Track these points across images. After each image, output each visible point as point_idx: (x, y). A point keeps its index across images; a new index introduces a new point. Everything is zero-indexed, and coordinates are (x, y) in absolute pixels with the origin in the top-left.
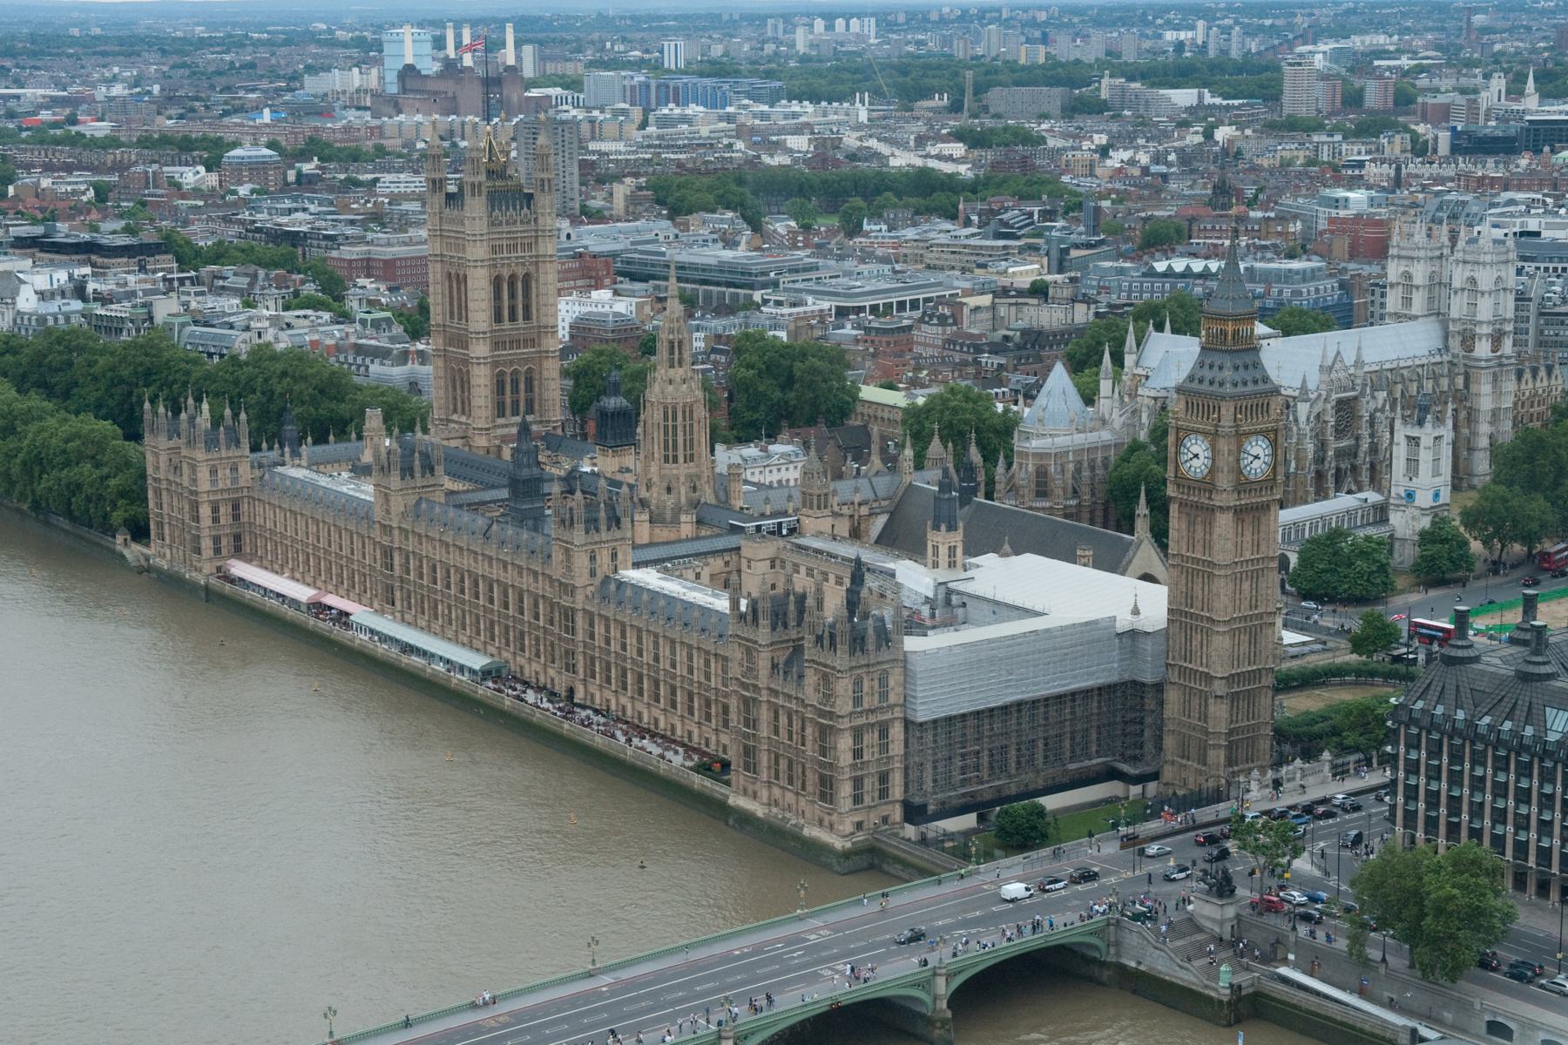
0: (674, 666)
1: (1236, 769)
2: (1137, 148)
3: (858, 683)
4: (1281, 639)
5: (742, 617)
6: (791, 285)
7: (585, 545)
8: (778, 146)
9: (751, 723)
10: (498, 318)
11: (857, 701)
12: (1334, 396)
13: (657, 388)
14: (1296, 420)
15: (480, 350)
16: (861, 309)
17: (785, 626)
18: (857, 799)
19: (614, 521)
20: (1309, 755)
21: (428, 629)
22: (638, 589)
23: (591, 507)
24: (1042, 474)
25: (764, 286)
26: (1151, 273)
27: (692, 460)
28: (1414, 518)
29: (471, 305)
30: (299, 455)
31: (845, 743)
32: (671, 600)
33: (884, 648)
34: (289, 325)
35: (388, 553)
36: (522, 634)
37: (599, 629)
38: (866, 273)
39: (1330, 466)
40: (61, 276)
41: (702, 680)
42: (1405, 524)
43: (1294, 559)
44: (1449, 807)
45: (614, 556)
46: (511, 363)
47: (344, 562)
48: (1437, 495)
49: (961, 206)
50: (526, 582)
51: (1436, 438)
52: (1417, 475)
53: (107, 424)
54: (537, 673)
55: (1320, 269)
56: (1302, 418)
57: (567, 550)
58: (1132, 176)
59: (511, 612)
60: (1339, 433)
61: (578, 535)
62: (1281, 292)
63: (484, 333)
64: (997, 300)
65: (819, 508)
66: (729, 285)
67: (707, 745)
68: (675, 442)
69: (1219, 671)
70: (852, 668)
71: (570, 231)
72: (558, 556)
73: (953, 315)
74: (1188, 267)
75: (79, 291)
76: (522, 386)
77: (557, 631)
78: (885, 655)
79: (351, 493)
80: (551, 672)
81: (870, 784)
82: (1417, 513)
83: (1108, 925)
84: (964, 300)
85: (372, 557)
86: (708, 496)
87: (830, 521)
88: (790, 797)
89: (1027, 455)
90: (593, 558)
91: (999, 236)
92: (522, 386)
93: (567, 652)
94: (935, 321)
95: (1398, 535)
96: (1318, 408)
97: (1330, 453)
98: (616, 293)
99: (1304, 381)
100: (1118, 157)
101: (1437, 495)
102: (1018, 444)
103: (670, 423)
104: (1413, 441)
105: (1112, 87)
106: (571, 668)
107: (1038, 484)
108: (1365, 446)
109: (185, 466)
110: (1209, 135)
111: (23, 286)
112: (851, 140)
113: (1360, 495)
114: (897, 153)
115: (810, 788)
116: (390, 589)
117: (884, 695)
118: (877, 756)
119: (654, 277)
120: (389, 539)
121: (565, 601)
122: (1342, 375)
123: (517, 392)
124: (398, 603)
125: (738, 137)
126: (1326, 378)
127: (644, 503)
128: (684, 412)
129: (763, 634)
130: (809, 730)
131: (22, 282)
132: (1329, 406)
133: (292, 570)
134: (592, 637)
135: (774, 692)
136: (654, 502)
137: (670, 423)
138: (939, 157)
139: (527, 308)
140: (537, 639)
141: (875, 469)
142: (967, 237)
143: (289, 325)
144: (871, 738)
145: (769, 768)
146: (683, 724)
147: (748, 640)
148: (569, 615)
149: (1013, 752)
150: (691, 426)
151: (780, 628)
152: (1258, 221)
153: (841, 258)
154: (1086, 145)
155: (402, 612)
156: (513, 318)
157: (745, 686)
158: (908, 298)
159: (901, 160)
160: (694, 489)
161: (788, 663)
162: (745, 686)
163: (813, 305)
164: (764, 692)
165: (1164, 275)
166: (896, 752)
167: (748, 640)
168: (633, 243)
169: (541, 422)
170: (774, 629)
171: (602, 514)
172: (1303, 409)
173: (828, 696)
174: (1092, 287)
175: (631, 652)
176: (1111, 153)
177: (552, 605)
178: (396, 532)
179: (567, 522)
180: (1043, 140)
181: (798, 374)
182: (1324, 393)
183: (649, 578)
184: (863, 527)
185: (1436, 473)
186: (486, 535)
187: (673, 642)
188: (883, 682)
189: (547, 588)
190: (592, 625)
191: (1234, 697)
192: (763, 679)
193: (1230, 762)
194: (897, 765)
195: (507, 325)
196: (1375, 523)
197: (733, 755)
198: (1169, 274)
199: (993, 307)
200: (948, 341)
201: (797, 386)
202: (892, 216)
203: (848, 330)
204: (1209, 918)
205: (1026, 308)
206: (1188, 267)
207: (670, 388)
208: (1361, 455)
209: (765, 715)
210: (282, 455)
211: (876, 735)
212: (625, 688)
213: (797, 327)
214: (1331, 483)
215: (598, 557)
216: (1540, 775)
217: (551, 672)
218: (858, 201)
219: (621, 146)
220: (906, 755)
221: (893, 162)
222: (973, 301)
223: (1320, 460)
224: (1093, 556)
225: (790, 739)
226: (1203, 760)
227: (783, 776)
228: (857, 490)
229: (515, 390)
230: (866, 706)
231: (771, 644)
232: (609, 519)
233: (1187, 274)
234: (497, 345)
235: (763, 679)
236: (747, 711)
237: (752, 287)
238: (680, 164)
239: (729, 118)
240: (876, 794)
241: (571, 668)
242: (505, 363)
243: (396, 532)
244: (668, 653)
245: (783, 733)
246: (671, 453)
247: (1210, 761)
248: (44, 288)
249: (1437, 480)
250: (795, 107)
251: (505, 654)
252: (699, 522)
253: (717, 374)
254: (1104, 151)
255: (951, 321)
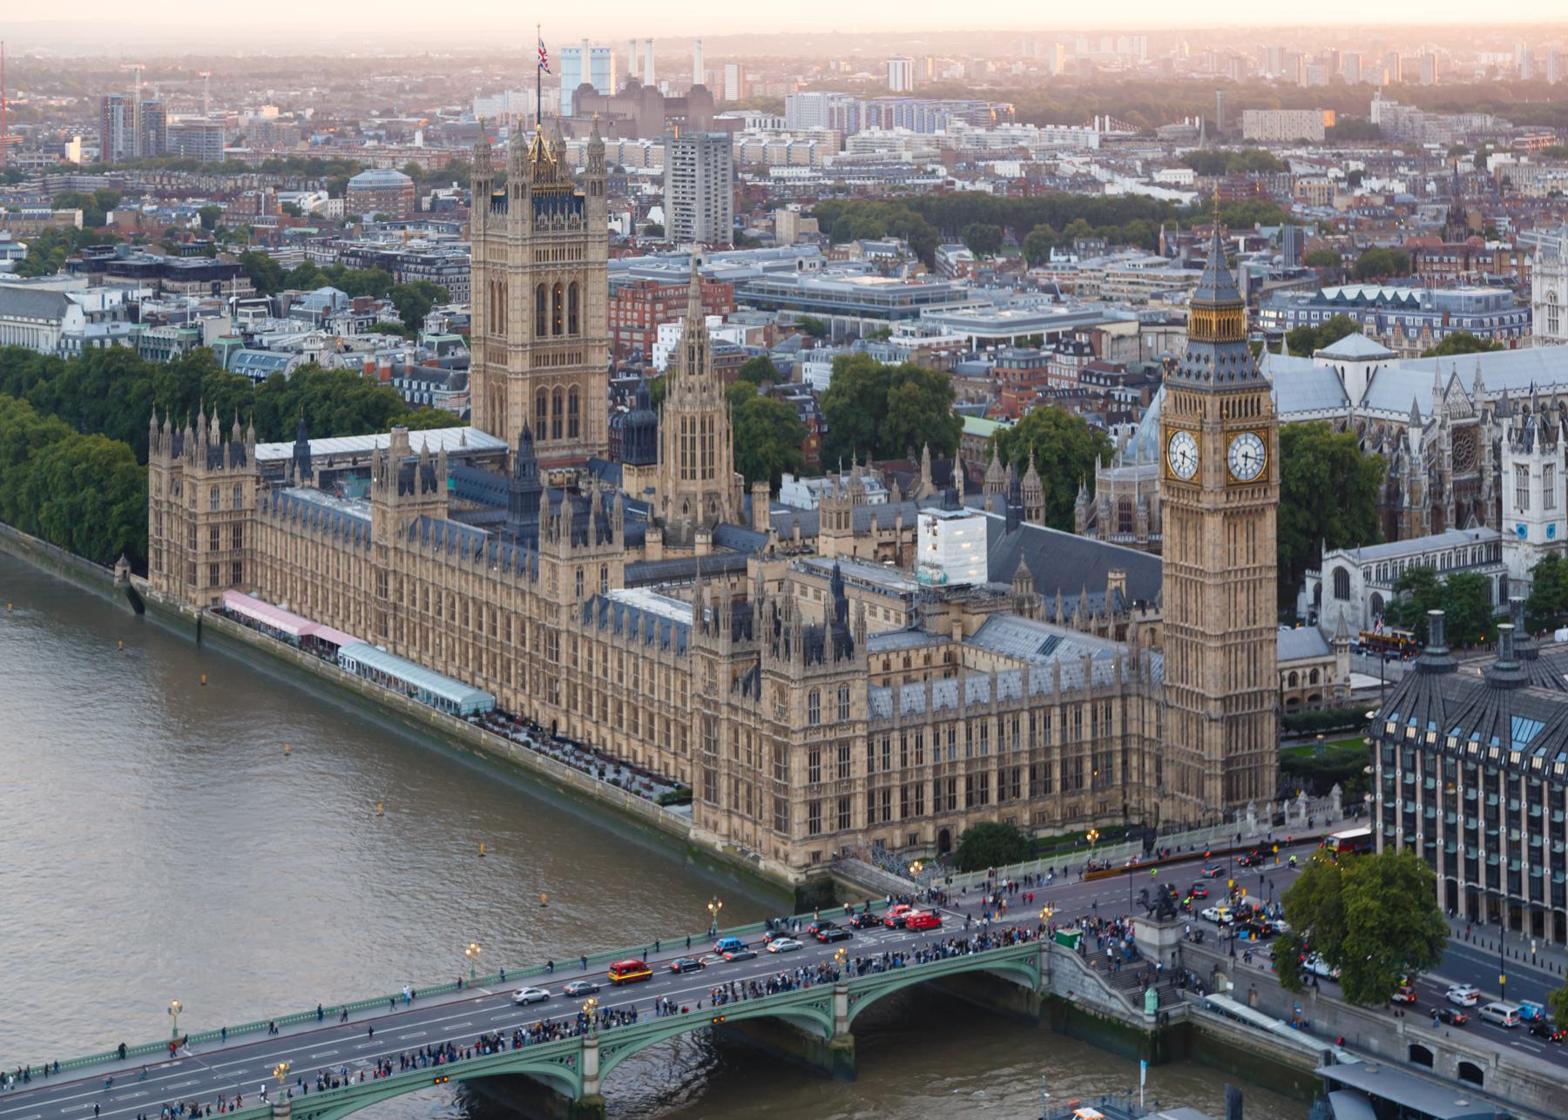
0: (652, 690)
1: (1238, 803)
2: (1392, 177)
3: (814, 697)
4: (1347, 679)
5: (705, 626)
6: (929, 315)
7: (571, 559)
8: (972, 173)
9: (712, 744)
10: (541, 330)
11: (814, 715)
12: (1449, 422)
13: (675, 396)
14: (1408, 448)
15: (518, 363)
16: (1006, 341)
17: (749, 637)
18: (814, 826)
19: (606, 534)
20: (1321, 791)
21: (418, 662)
22: (620, 606)
23: (580, 518)
24: (1125, 508)
25: (903, 316)
26: (1320, 300)
27: (712, 476)
28: (1527, 556)
29: (510, 315)
30: (311, 475)
31: (798, 762)
32: (650, 617)
33: (844, 658)
34: (347, 349)
35: (382, 576)
36: (509, 661)
37: (582, 653)
38: (1021, 302)
39: (1449, 503)
40: (115, 297)
41: (679, 704)
42: (1519, 561)
43: (1387, 596)
44: (1425, 832)
45: (604, 574)
46: (554, 379)
47: (340, 590)
48: (1551, 531)
49: (1162, 236)
50: (514, 603)
51: (1548, 466)
52: (1527, 507)
53: (117, 443)
54: (522, 706)
55: (1506, 297)
56: (1415, 446)
57: (553, 565)
58: (1373, 207)
59: (498, 638)
60: (1459, 463)
61: (563, 549)
62: (1460, 323)
63: (524, 345)
64: (1144, 329)
65: (839, 527)
66: (864, 314)
67: (683, 778)
68: (693, 456)
69: (1212, 691)
70: (806, 679)
71: (700, 256)
72: (544, 571)
73: (1090, 344)
74: (1361, 294)
75: (132, 313)
76: (566, 405)
77: (542, 656)
78: (845, 665)
79: (357, 514)
80: (536, 704)
81: (827, 810)
82: (1530, 550)
83: (1041, 951)
84: (1102, 328)
85: (369, 583)
86: (727, 513)
87: (851, 542)
88: (748, 826)
89: (1108, 485)
90: (580, 575)
91: (1189, 265)
92: (566, 405)
93: (550, 680)
94: (1071, 350)
95: (1512, 575)
96: (1434, 433)
97: (1449, 486)
98: (725, 320)
99: (1415, 405)
100: (1370, 184)
101: (1551, 531)
102: (1099, 474)
103: (688, 435)
104: (1522, 469)
105: (1383, 112)
106: (554, 698)
107: (1121, 517)
108: (1489, 481)
109: (186, 486)
110: (1481, 162)
111: (70, 307)
112: (1069, 165)
113: (1473, 532)
114: (1117, 178)
115: (766, 815)
116: (383, 618)
117: (844, 711)
118: (836, 778)
119: (781, 306)
120: (383, 561)
121: (550, 623)
122: (1460, 398)
123: (560, 412)
124: (391, 634)
125: (941, 163)
126: (1440, 400)
127: (658, 523)
128: (703, 424)
129: (723, 645)
130: (765, 749)
131: (71, 302)
132: (1444, 433)
133: (291, 601)
134: (575, 663)
135: (734, 709)
136: (669, 521)
137: (688, 435)
138: (1163, 185)
139: (573, 320)
140: (523, 667)
141: (924, 494)
142: (1146, 266)
143: (347, 349)
144: (828, 758)
145: (729, 795)
146: (660, 756)
147: (710, 652)
148: (553, 637)
149: (993, 781)
150: (712, 438)
151: (743, 639)
152: (1490, 253)
153: (1002, 286)
154: (1334, 172)
155: (394, 643)
156: (557, 329)
157: (706, 703)
158: (1060, 330)
159: (1121, 187)
160: (714, 508)
161: (749, 679)
162: (706, 703)
163: (949, 336)
164: (725, 709)
165: (1334, 303)
166: (858, 775)
167: (710, 652)
168: (766, 269)
169: (586, 446)
170: (735, 639)
171: (592, 526)
172: (1415, 435)
173: (783, 712)
174: (1269, 319)
175: (612, 677)
176: (1363, 182)
177: (538, 627)
178: (391, 554)
179: (553, 537)
180: (1286, 166)
181: (891, 401)
182: (1439, 419)
183: (641, 598)
184: (905, 555)
185: (1548, 505)
186: (478, 554)
187: (652, 663)
188: (844, 695)
189: (535, 609)
190: (575, 649)
191: (1231, 723)
192: (723, 697)
193: (1229, 795)
194: (859, 789)
195: (550, 337)
196: (1489, 563)
197: (693, 777)
198: (1340, 300)
199: (1140, 335)
200: (1085, 373)
201: (890, 415)
202: (1082, 245)
203: (984, 361)
204: (1150, 945)
205: (1176, 338)
206: (1361, 294)
207: (689, 397)
208: (1486, 489)
209: (724, 734)
210: (292, 475)
211: (836, 754)
212: (605, 719)
213: (920, 358)
214: (1450, 518)
215: (586, 574)
216: (1507, 790)
217: (536, 704)
218: (1047, 229)
219: (805, 172)
220: (870, 779)
221: (1110, 190)
222: (1115, 330)
223: (1436, 491)
224: (1128, 580)
225: (749, 761)
226: (1200, 792)
227: (742, 803)
228: (899, 513)
229: (558, 409)
230: (823, 721)
231: (733, 656)
232: (599, 532)
233: (1360, 301)
234: (537, 359)
235: (723, 697)
236: (709, 731)
237: (887, 316)
238: (862, 190)
239: (938, 142)
240: (836, 822)
241: (554, 698)
242: (546, 381)
243: (391, 554)
244: (647, 676)
245: (743, 756)
246: (688, 468)
247: (1206, 794)
248: (94, 309)
249: (1550, 513)
250: (1017, 130)
251: (493, 686)
252: (716, 542)
253: (815, 407)
254: (1354, 179)
255: (1087, 350)
